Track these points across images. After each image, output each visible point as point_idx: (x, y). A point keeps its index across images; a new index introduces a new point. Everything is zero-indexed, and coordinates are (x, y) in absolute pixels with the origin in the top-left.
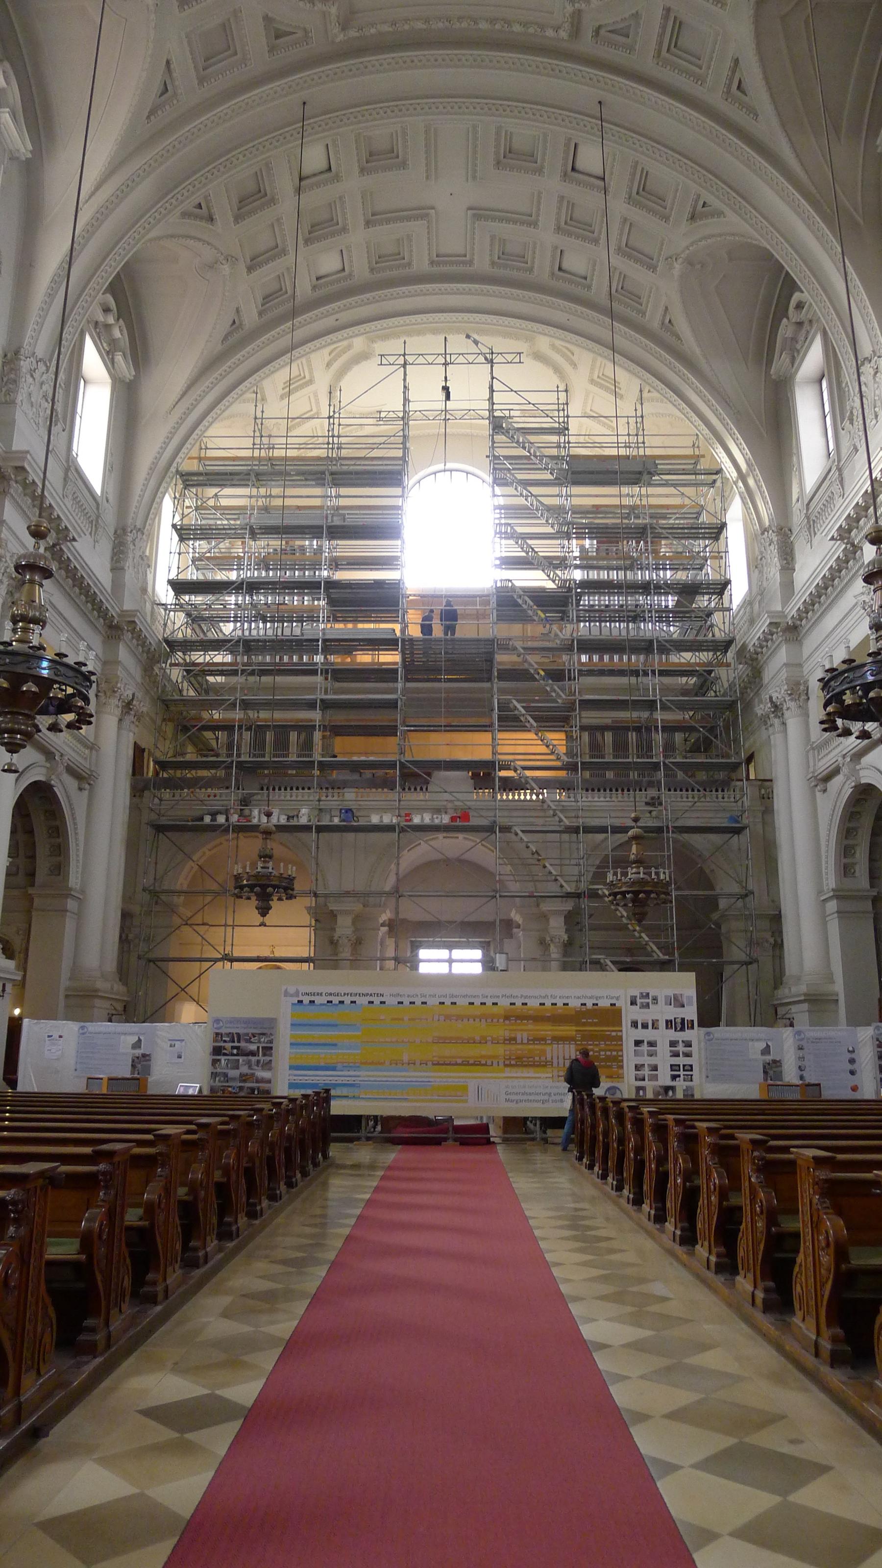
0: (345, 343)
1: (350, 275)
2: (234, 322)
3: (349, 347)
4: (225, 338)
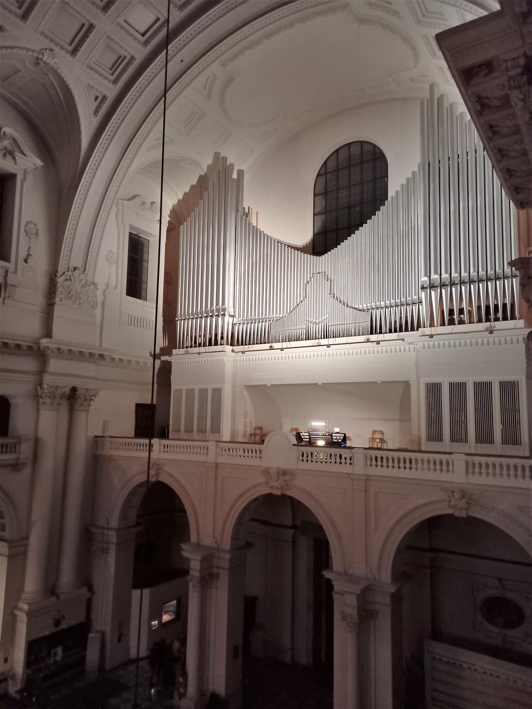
3: (215, 77)
4: (96, 112)
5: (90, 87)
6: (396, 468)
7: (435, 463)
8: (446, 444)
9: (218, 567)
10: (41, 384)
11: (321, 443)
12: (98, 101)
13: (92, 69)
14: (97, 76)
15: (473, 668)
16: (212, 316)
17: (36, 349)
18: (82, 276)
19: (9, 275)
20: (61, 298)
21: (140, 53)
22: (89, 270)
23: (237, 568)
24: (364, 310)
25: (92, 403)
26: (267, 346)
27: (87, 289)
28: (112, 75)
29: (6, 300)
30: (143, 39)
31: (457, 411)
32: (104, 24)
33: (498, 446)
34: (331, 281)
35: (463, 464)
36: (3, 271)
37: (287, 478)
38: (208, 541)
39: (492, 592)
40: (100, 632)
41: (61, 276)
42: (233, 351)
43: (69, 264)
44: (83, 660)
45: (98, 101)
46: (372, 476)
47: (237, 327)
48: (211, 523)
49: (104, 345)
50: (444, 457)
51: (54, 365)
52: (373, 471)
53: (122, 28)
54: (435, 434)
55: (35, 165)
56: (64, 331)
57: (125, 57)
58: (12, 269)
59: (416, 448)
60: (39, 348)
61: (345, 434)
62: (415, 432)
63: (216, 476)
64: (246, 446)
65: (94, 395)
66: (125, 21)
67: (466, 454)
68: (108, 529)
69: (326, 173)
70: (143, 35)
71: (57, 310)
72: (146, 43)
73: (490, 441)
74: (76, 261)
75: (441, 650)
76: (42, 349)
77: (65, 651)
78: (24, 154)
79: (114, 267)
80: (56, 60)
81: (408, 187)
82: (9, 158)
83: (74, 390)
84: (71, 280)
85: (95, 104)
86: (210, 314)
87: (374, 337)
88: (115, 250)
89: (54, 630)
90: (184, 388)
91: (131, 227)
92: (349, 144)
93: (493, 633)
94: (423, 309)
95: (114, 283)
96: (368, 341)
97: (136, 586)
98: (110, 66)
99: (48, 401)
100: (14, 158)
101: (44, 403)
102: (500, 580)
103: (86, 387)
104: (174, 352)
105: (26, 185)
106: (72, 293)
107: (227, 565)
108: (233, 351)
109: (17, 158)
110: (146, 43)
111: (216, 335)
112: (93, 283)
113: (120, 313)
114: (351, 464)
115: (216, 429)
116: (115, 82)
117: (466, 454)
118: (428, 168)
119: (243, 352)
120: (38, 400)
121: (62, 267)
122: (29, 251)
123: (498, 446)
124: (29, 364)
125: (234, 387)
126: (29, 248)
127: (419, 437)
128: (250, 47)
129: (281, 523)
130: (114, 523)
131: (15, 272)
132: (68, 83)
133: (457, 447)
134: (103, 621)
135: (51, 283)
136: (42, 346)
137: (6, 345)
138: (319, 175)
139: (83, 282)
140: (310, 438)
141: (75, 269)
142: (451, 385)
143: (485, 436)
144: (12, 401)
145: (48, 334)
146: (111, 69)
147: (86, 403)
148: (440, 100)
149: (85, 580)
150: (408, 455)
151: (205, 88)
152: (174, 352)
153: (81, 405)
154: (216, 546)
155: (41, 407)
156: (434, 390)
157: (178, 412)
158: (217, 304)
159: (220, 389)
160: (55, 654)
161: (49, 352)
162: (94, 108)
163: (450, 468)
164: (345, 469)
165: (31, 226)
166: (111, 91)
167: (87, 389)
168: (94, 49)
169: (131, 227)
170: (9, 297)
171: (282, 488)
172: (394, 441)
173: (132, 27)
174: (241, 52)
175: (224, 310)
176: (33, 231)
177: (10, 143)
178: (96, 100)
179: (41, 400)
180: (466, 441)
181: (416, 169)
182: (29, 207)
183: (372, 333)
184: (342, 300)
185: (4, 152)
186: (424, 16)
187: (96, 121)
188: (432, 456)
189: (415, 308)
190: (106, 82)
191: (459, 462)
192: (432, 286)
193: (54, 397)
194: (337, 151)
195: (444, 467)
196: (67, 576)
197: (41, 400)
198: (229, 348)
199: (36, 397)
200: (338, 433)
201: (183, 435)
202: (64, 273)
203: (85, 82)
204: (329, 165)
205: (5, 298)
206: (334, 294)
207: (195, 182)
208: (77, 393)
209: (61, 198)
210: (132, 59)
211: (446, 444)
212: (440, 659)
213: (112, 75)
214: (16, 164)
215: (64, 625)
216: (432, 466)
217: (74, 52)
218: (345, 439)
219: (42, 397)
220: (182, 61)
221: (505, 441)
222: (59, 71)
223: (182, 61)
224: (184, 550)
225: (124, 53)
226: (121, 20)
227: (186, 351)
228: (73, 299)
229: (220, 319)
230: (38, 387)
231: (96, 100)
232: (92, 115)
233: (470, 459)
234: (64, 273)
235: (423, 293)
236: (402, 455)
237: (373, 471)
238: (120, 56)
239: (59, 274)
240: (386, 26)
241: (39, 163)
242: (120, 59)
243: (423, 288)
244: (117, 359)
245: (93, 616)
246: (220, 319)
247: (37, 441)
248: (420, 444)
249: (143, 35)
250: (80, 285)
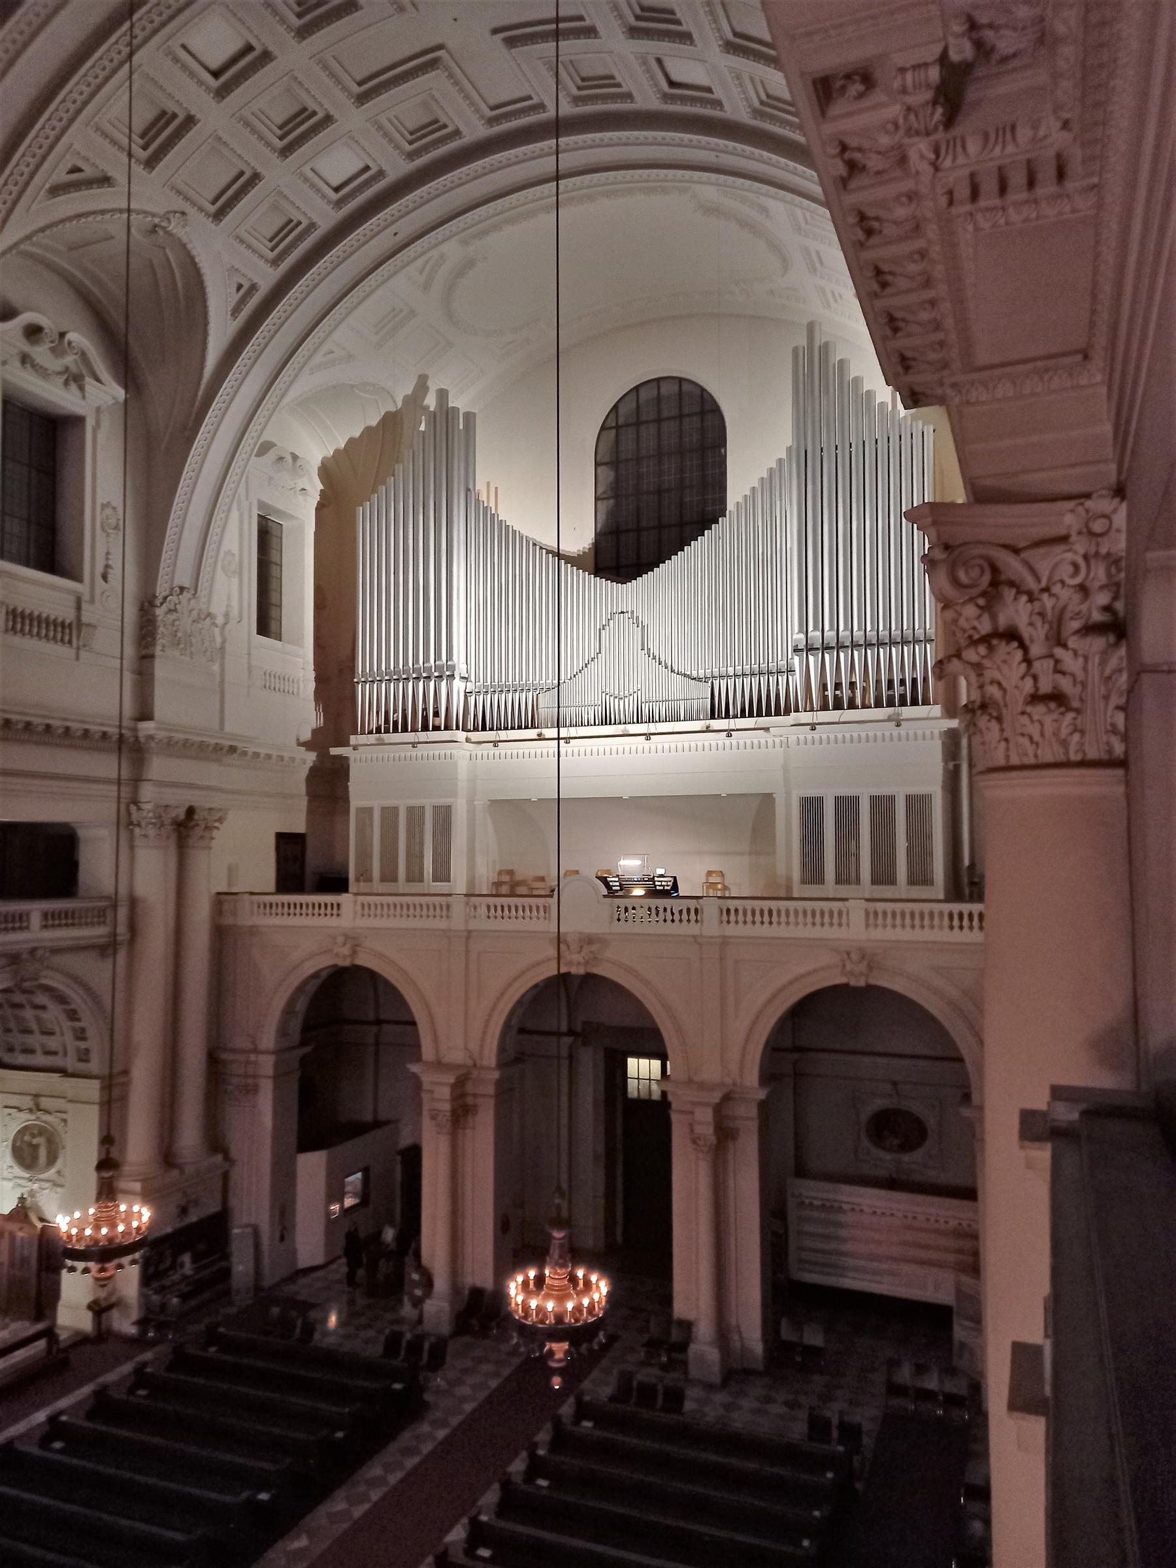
0: (435, 253)
1: (381, 174)
2: (240, 287)
4: (236, 311)
6: (766, 924)
7: (822, 914)
8: (830, 886)
9: (475, 1096)
10: (136, 802)
11: (639, 892)
13: (242, 241)
14: (248, 253)
15: (857, 1208)
16: (428, 678)
17: (132, 740)
18: (192, 602)
19: (85, 606)
20: (164, 646)
21: (326, 218)
22: (202, 592)
23: (504, 1092)
24: (699, 679)
25: (215, 833)
26: (532, 733)
27: (200, 626)
28: (272, 250)
29: (83, 654)
30: (334, 196)
31: (837, 835)
33: (902, 887)
34: (643, 627)
35: (862, 914)
36: (72, 598)
37: (594, 948)
38: (457, 1056)
40: (247, 1226)
41: (162, 604)
42: (468, 740)
43: (172, 580)
44: (226, 1274)
46: (731, 937)
47: (473, 698)
48: (459, 1024)
49: (228, 728)
50: (836, 906)
51: (158, 767)
52: (731, 930)
53: (306, 179)
54: (813, 872)
55: (114, 398)
56: (170, 707)
57: (299, 223)
58: (86, 597)
59: (783, 895)
60: (137, 737)
61: (675, 878)
62: (781, 870)
63: (467, 951)
64: (492, 901)
65: (220, 820)
67: (868, 900)
68: (256, 1051)
70: (337, 190)
71: (162, 670)
72: (339, 204)
73: (892, 881)
74: (183, 577)
75: (812, 1190)
76: (142, 740)
77: (195, 1260)
78: (98, 380)
79: (235, 581)
80: (188, 229)
81: (770, 483)
82: (73, 387)
83: (191, 811)
84: (175, 610)
86: (424, 675)
87: (717, 724)
88: (236, 551)
89: (179, 1225)
90: (377, 805)
91: (262, 505)
93: (885, 1160)
94: (797, 679)
95: (235, 612)
96: (708, 730)
97: (306, 1144)
98: (269, 234)
99: (152, 831)
100: (81, 388)
101: (146, 836)
102: (895, 1084)
103: (208, 806)
104: (353, 739)
105: (101, 436)
106: (179, 634)
107: (490, 1090)
108: (468, 740)
109: (87, 388)
110: (339, 204)
111: (425, 709)
112: (209, 615)
113: (250, 668)
114: (697, 921)
115: (442, 873)
116: (275, 262)
117: (868, 900)
118: (805, 458)
119: (495, 743)
120: (132, 832)
121: (161, 590)
122: (107, 559)
123: (902, 887)
124: (106, 765)
125: (471, 802)
126: (108, 553)
127: (789, 879)
129: (576, 1021)
130: (268, 1039)
131: (92, 601)
132: (200, 265)
133: (843, 891)
134: (252, 1208)
135: (142, 616)
136: (141, 735)
137: (7, 722)
138: (603, 428)
139: (195, 613)
140: (621, 885)
141: (182, 589)
142: (837, 799)
143: (883, 875)
144: (82, 833)
145: (145, 713)
146: (271, 240)
147: (207, 834)
148: (825, 349)
149: (215, 1141)
150: (766, 905)
152: (353, 739)
153: (202, 837)
154: (470, 1063)
155: (137, 842)
156: (811, 808)
157: (358, 845)
158: (438, 656)
159: (450, 807)
160: (182, 1266)
161: (153, 744)
163: (844, 920)
164: (693, 929)
165: (108, 511)
166: (266, 277)
167: (210, 809)
168: (255, 215)
170: (85, 646)
171: (587, 963)
172: (740, 883)
173: (319, 176)
174: (497, 227)
175: (452, 668)
176: (113, 521)
177: (76, 361)
178: (238, 289)
179: (137, 831)
180: (858, 882)
181: (783, 455)
182: (102, 478)
183: (713, 717)
184: (662, 660)
185: (65, 377)
186: (807, 223)
187: (233, 327)
188: (809, 905)
189: (782, 680)
190: (261, 263)
191: (856, 910)
192: (810, 649)
193: (162, 825)
195: (836, 920)
196: (190, 1137)
197: (137, 831)
198: (461, 735)
199: (126, 824)
200: (662, 876)
201: (377, 885)
202: (165, 598)
203: (227, 262)
205: (78, 649)
206: (649, 650)
208: (196, 817)
209: (159, 459)
211: (830, 886)
212: (811, 1204)
213: (272, 250)
214: (84, 397)
215: (193, 1218)
216: (809, 919)
218: (675, 886)
219: (139, 825)
220: (395, 234)
221: (912, 882)
222: (189, 246)
223: (395, 234)
225: (296, 216)
227: (377, 739)
228: (182, 646)
229: (444, 684)
230: (133, 808)
233: (872, 906)
234: (165, 598)
235: (796, 659)
236: (758, 904)
237: (731, 930)
238: (291, 221)
239: (158, 602)
240: (744, 224)
241: (120, 393)
242: (289, 225)
243: (796, 650)
244: (250, 753)
245: (233, 1202)
246: (444, 684)
247: (133, 902)
248: (789, 888)
249: (337, 190)
250: (190, 620)
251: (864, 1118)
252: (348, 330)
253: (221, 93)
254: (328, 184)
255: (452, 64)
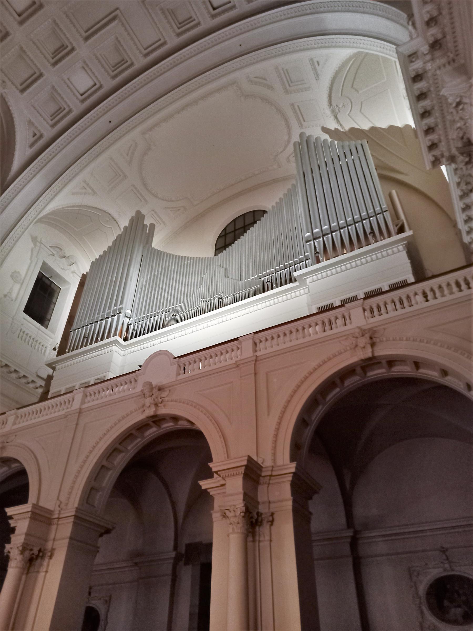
2: (35, 135)
4: (31, 146)
5: (30, 123)
12: (36, 137)
21: (77, 108)
30: (81, 98)
32: (51, 76)
39: (435, 572)
45: (36, 137)
53: (65, 82)
66: (68, 79)
69: (225, 235)
70: (82, 95)
79: (17, 286)
80: (6, 91)
85: (33, 139)
88: (23, 273)
91: (44, 264)
92: (244, 215)
110: (83, 101)
128: (165, 120)
132: (12, 112)
138: (220, 237)
151: (127, 155)
162: (30, 142)
166: (48, 133)
168: (39, 91)
169: (44, 264)
173: (74, 86)
178: (34, 136)
187: (29, 152)
190: (45, 123)
194: (234, 221)
204: (227, 229)
207: (110, 244)
210: (70, 111)
217: (23, 91)
222: (6, 99)
224: (11, 517)
226: (65, 78)
231: (34, 136)
232: (27, 146)
249: (82, 95)
251: (422, 588)
252: (90, 171)
253: (21, 23)
254: (78, 92)
255: (123, 19)
